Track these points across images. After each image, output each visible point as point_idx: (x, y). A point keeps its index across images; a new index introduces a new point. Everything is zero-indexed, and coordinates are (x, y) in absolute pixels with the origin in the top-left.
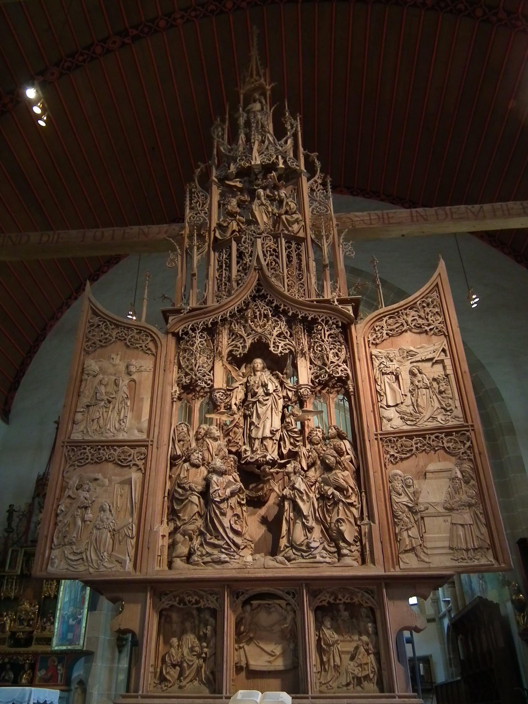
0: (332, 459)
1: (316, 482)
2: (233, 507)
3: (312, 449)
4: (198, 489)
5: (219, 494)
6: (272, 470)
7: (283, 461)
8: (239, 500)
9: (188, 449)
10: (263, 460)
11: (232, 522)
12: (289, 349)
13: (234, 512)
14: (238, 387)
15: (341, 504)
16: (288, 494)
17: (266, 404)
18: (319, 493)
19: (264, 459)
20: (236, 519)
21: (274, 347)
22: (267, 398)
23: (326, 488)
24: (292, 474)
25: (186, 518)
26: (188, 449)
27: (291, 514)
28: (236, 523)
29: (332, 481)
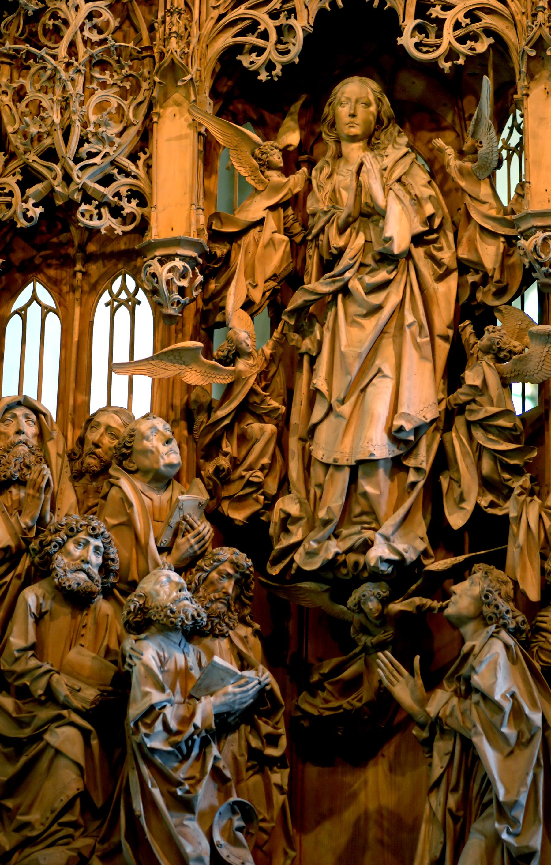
2: (228, 773)
4: (83, 700)
5: (165, 725)
9: (41, 521)
11: (217, 837)
12: (489, 32)
13: (228, 795)
14: (261, 222)
17: (379, 308)
21: (420, 29)
22: (382, 275)
25: (34, 817)
26: (41, 521)
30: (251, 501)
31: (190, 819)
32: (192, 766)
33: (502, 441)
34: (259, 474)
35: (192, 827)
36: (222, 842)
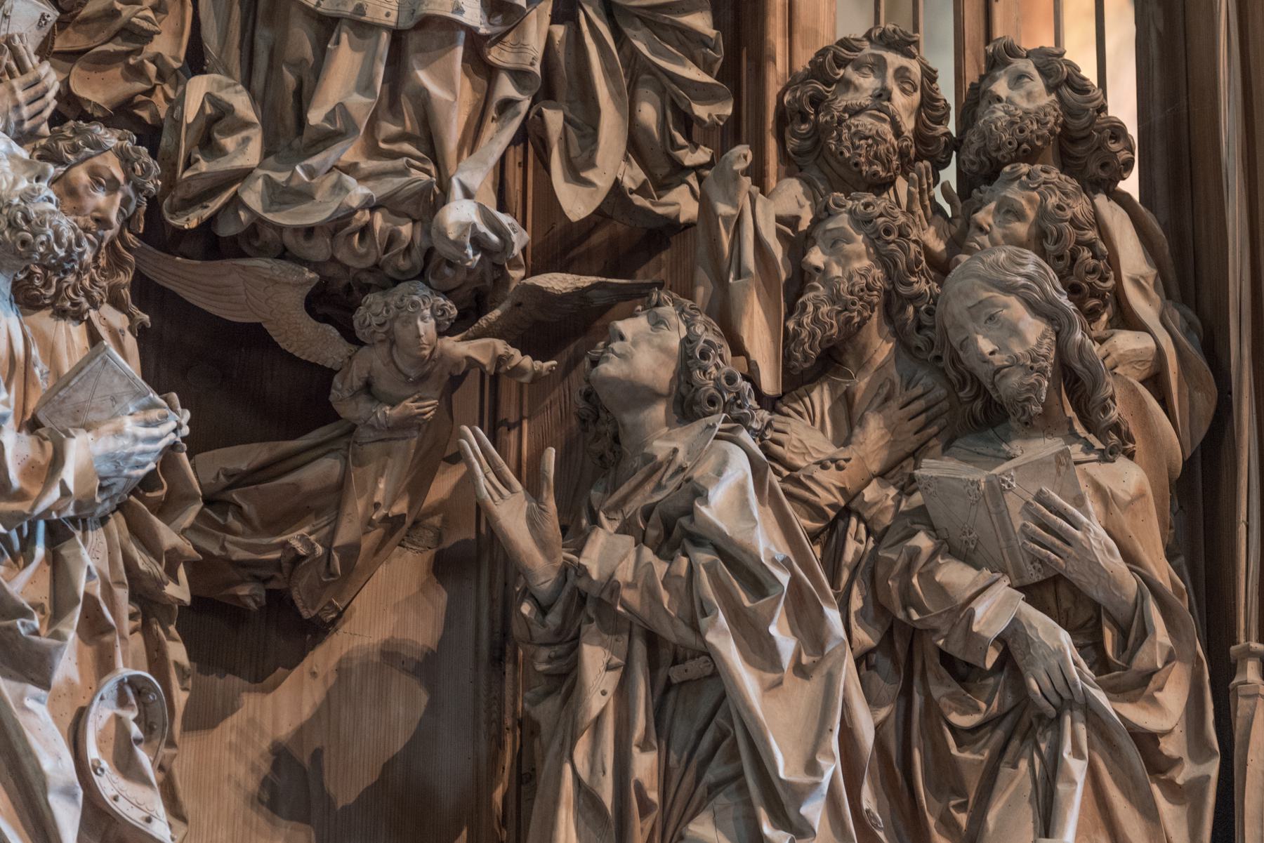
0: (1033, 329)
1: (845, 512)
3: (842, 221)
6: (457, 347)
7: (557, 282)
8: (143, 562)
10: (393, 238)
11: (93, 753)
13: (104, 665)
15: (1075, 730)
16: (625, 573)
18: (878, 610)
19: (406, 229)
20: (135, 731)
23: (956, 575)
24: (659, 411)
27: (645, 765)
28: (127, 766)
29: (1018, 522)
30: (116, 71)
31: (38, 700)
32: (32, 581)
33: (689, 63)
34: (150, 14)
35: (42, 717)
36: (105, 764)
